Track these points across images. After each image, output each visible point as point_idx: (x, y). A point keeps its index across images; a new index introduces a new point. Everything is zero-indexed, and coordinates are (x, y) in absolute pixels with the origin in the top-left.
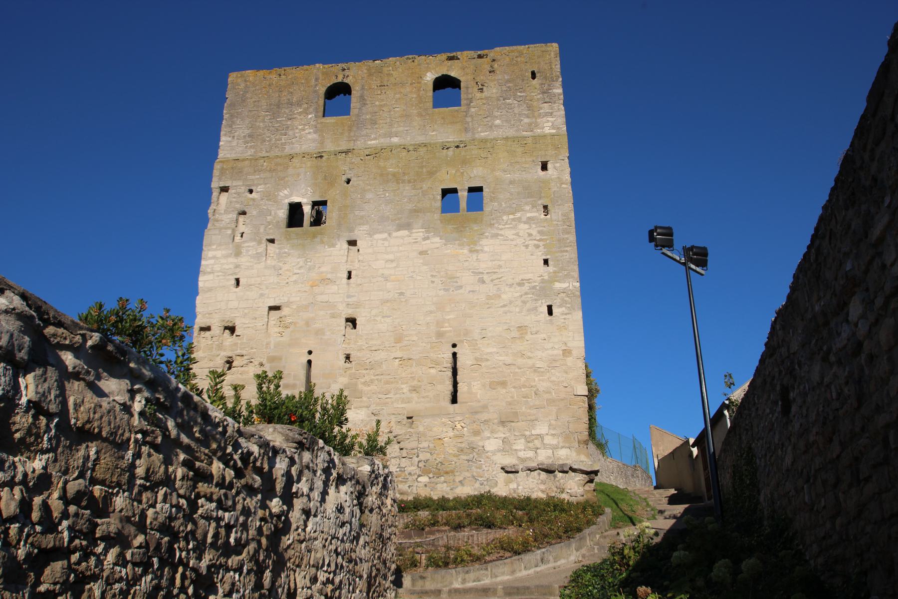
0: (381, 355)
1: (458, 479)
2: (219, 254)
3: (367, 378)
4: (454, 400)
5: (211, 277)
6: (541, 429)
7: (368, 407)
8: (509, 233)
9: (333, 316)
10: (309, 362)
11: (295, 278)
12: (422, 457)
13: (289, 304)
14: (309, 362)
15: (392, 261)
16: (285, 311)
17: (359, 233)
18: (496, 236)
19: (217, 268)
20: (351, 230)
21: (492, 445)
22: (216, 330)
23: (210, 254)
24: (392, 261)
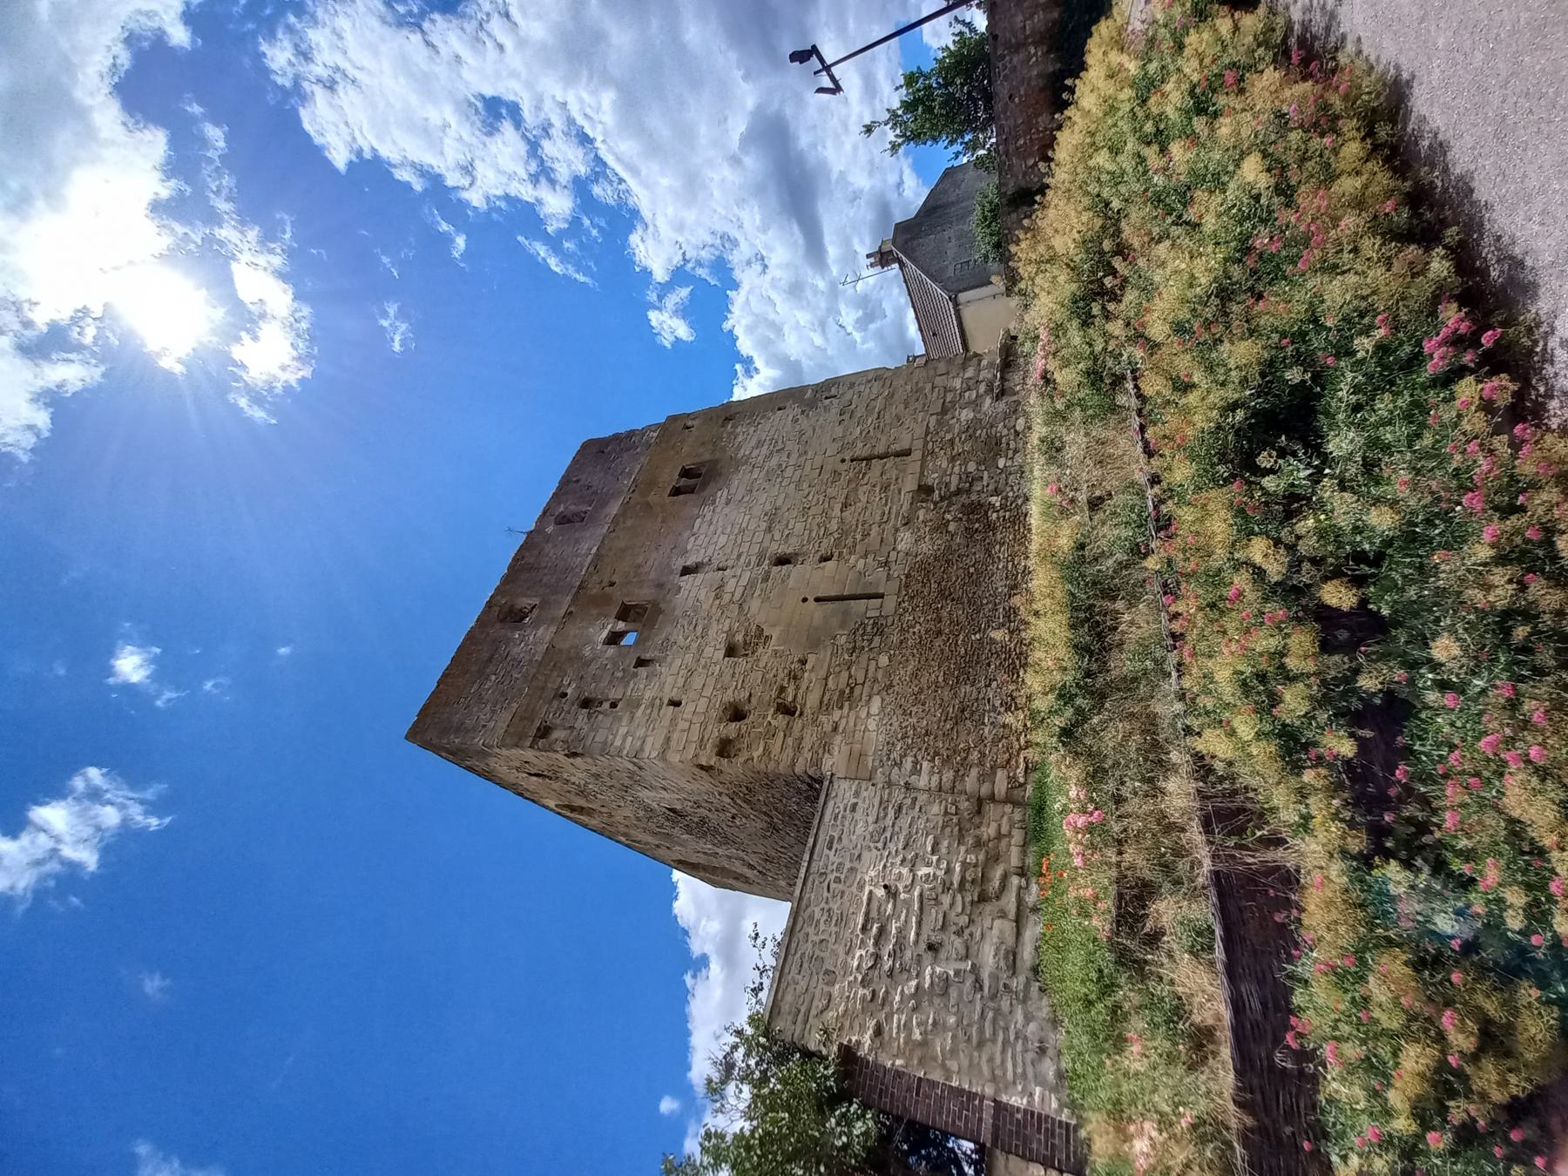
0: (834, 525)
1: (1005, 432)
2: (623, 730)
3: (859, 537)
4: (907, 453)
5: (650, 740)
6: (957, 383)
7: (897, 530)
8: (740, 439)
9: (765, 579)
10: (817, 600)
11: (699, 629)
12: (972, 467)
13: (730, 633)
14: (817, 600)
15: (724, 528)
16: (739, 638)
17: (679, 563)
18: (739, 448)
19: (641, 732)
20: (672, 572)
21: (966, 415)
22: (732, 729)
23: (618, 743)
24: (724, 528)
